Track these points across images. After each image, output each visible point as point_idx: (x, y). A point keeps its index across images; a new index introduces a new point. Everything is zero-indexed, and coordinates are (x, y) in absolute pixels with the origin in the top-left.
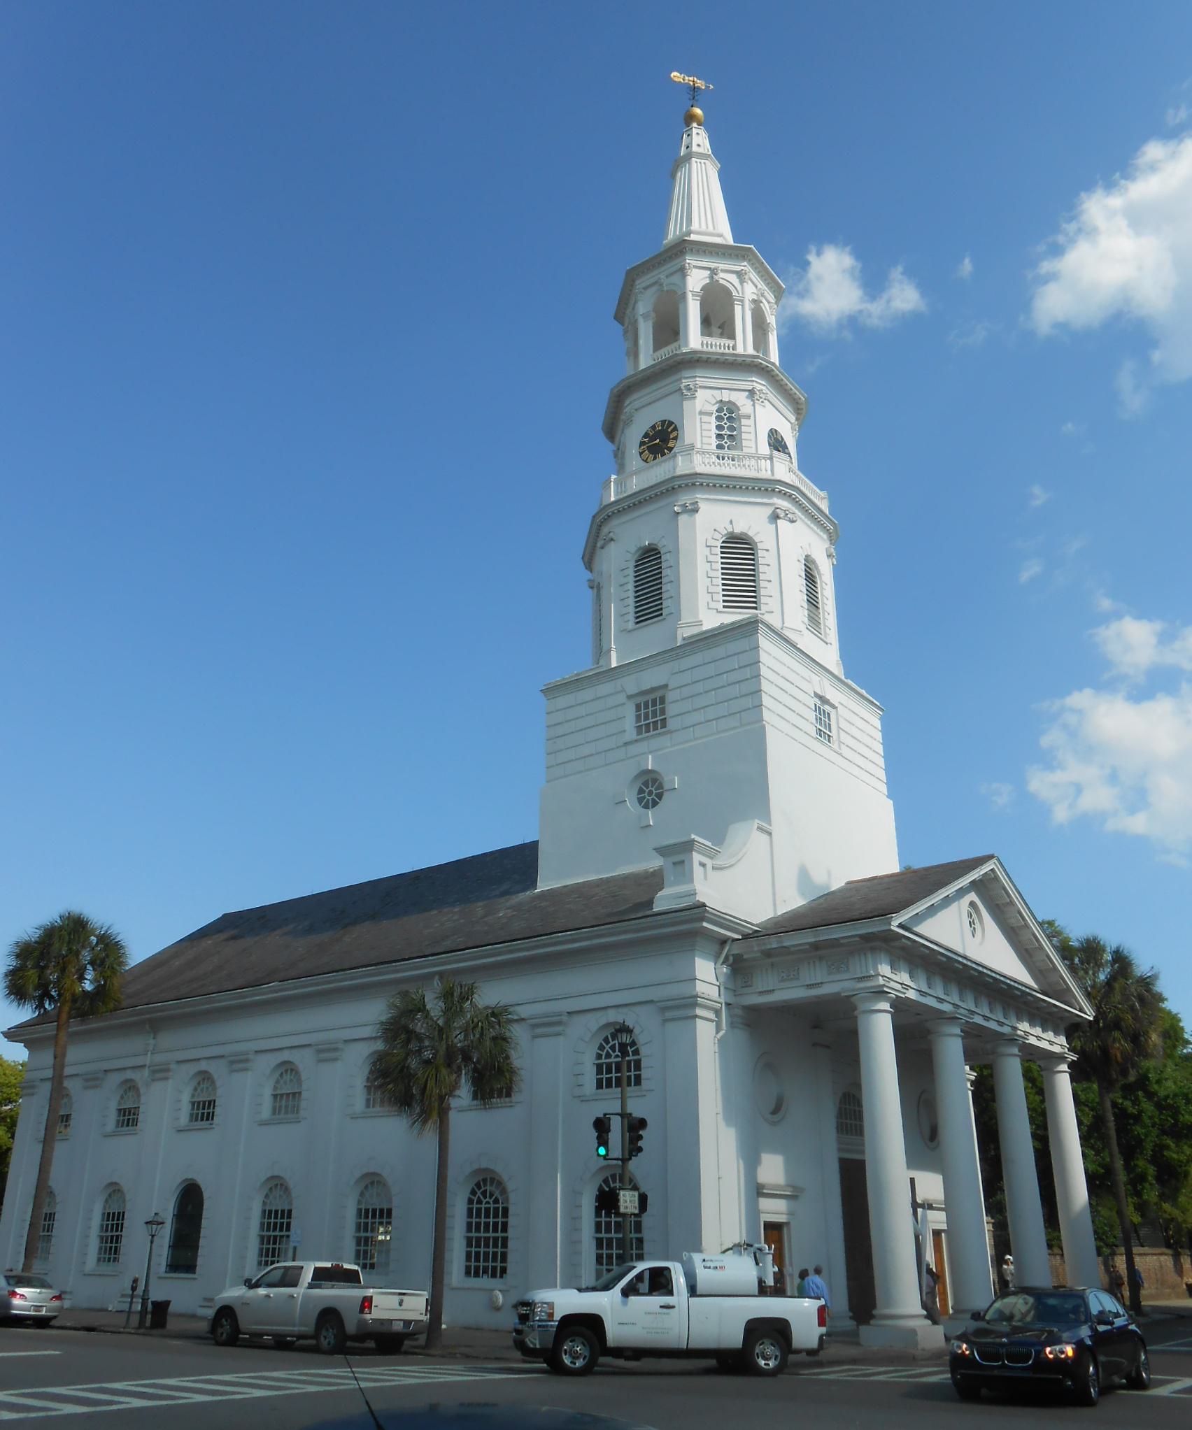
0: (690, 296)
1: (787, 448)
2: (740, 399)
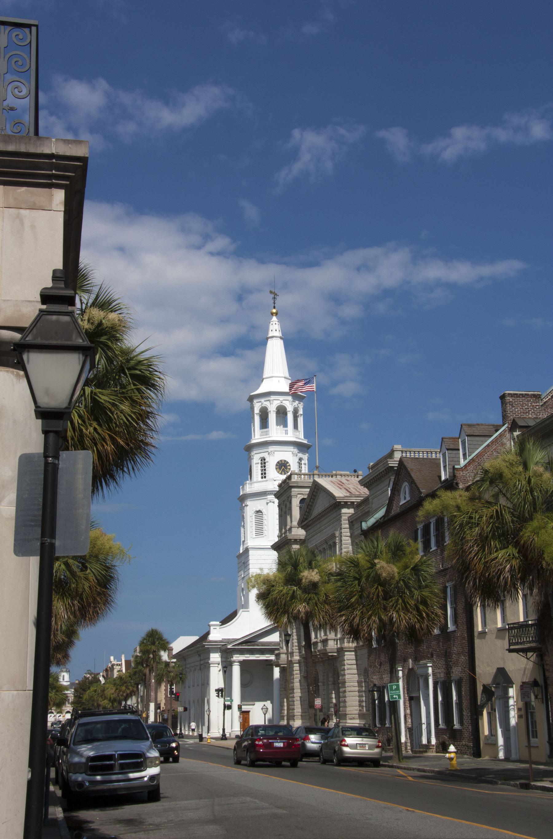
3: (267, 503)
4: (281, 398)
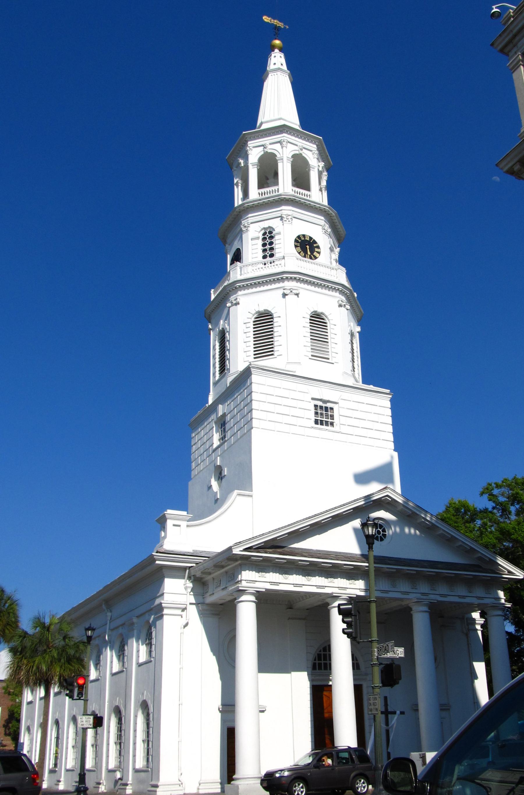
2: (275, 224)
3: (284, 295)
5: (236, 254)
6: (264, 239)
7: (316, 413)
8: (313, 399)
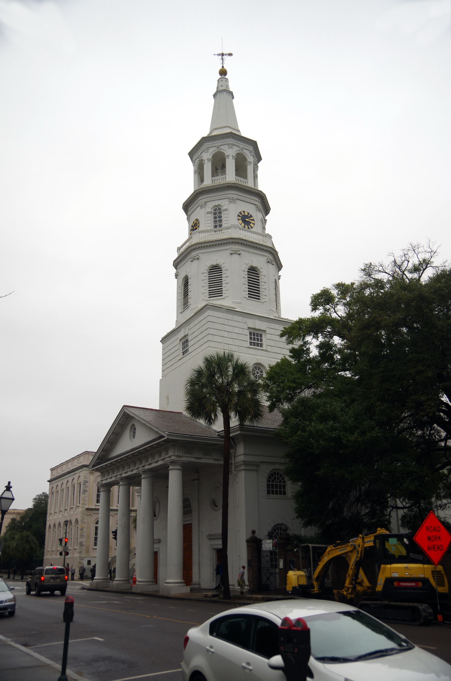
0: (206, 161)
1: (252, 217)
2: (225, 204)
4: (242, 145)
5: (195, 223)
6: (215, 214)
7: (251, 338)
8: (249, 328)
